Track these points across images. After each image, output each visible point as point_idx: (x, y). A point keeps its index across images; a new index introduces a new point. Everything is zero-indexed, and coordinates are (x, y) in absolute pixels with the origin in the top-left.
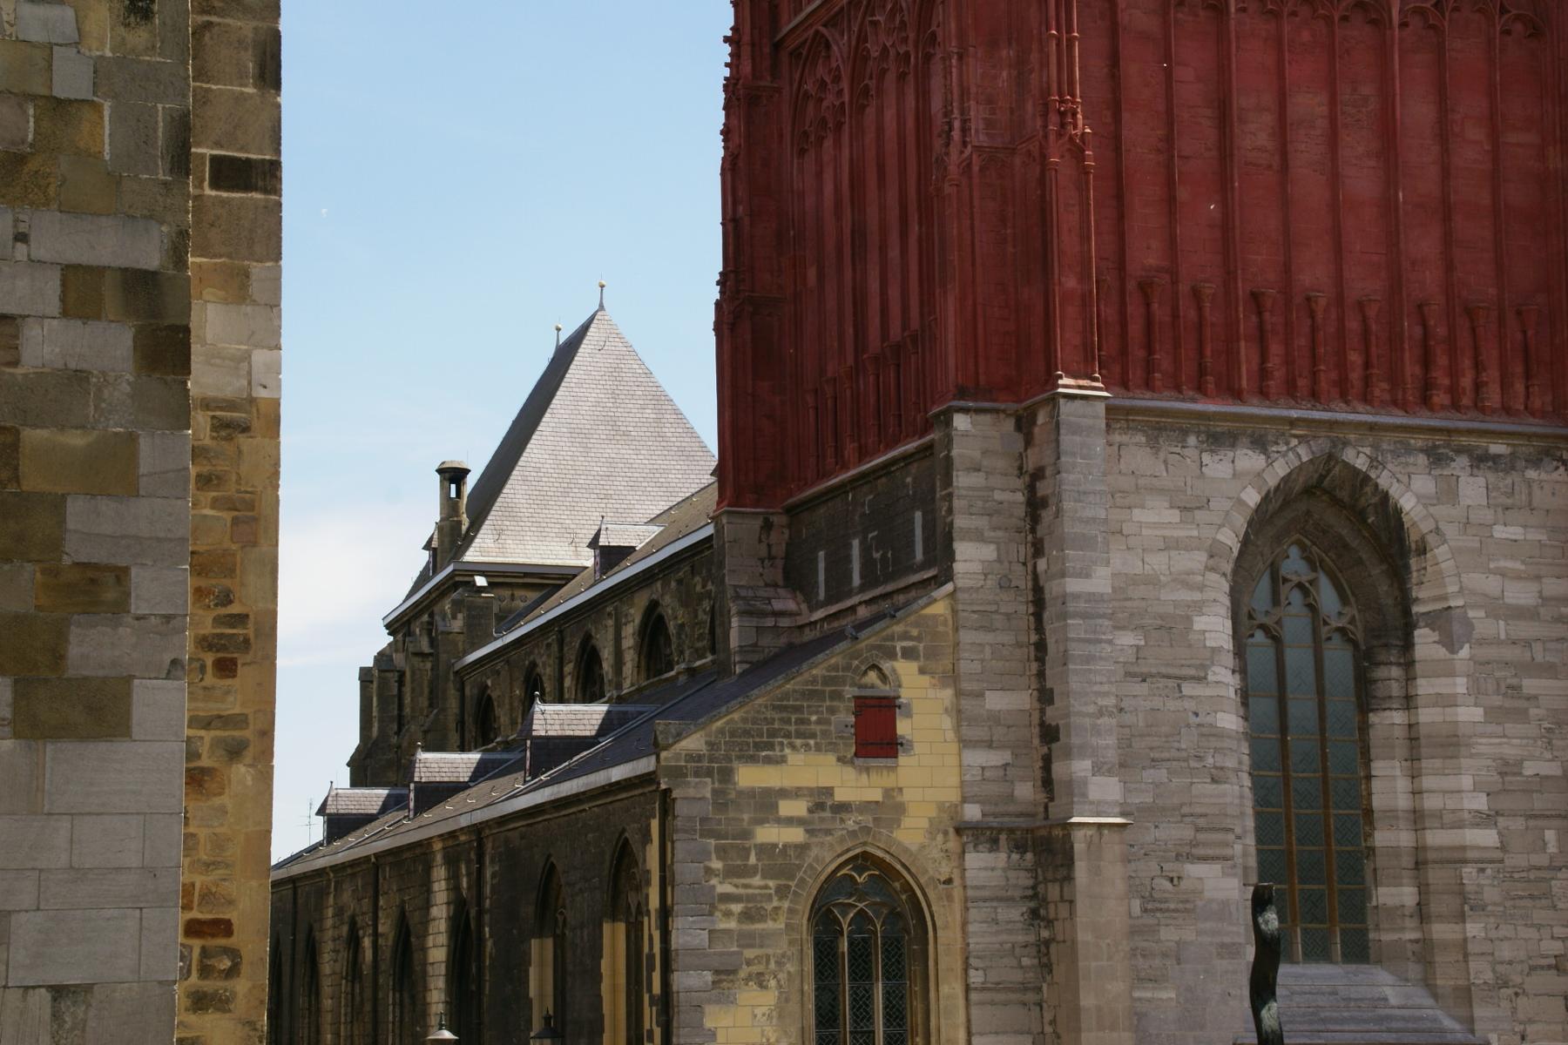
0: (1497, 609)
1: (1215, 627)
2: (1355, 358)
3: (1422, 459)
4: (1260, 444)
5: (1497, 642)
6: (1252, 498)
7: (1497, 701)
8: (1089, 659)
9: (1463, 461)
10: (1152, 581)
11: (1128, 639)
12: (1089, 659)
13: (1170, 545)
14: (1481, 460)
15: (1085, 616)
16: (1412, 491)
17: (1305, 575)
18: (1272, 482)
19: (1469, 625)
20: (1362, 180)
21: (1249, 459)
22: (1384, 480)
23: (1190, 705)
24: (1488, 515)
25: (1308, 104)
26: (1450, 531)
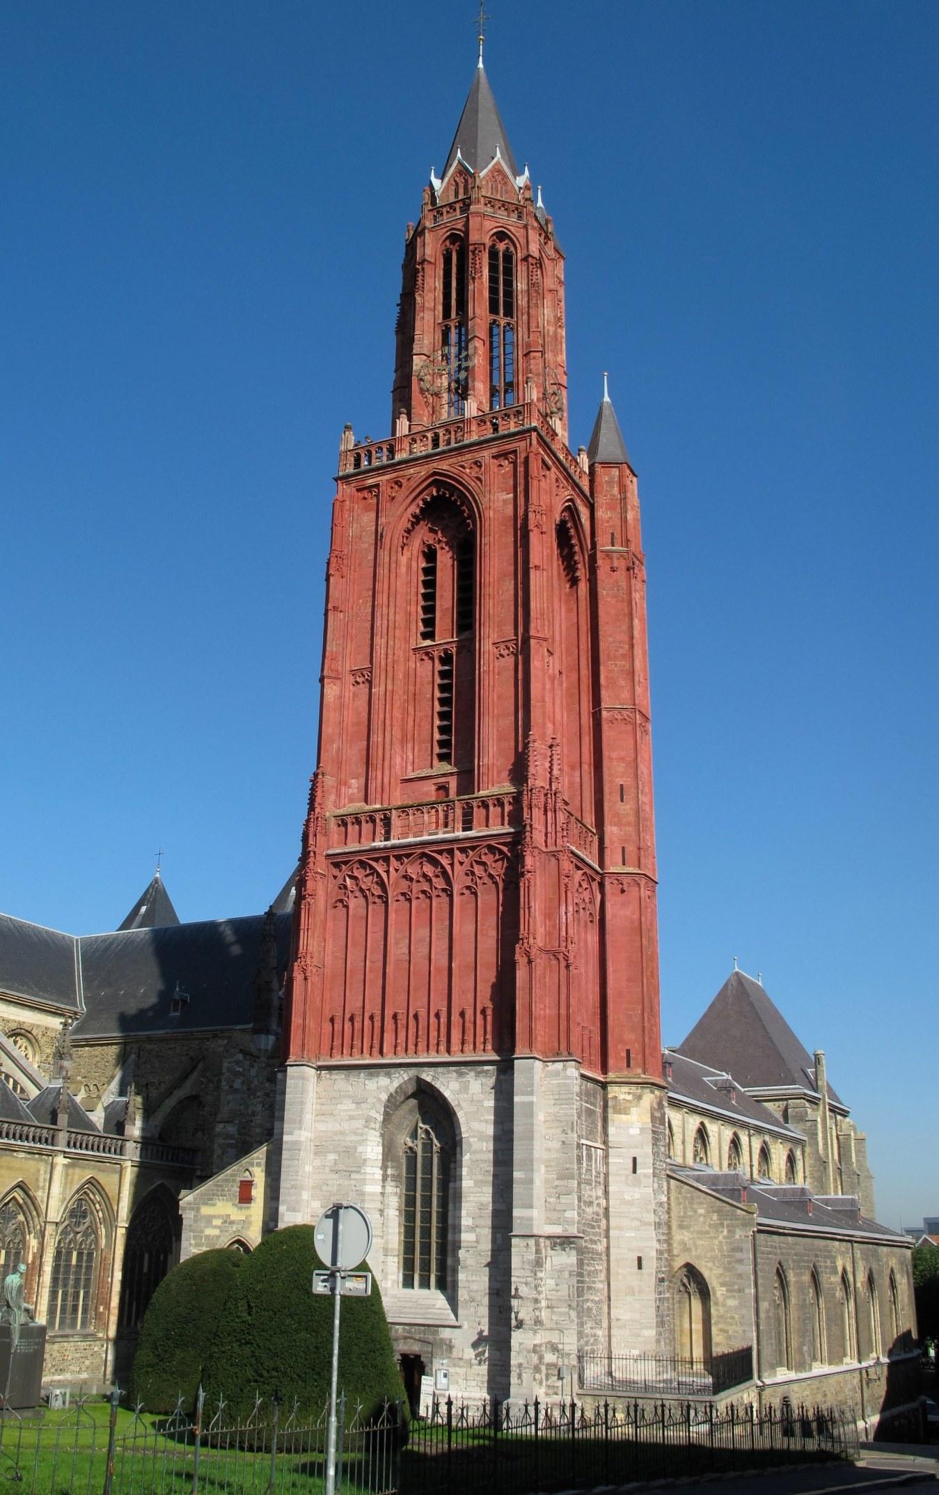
0: (481, 1137)
1: (373, 1150)
2: (433, 1034)
3: (455, 1075)
4: (388, 1075)
5: (482, 1151)
6: (384, 1097)
7: (480, 1177)
8: (289, 1166)
9: (472, 1074)
10: (342, 1133)
11: (332, 1157)
12: (289, 1166)
13: (351, 1118)
14: (478, 1074)
15: (289, 1150)
16: (449, 1086)
17: (427, 1127)
18: (392, 1090)
19: (470, 1145)
20: (440, 960)
21: (383, 1081)
22: (438, 1085)
23: (353, 1182)
24: (482, 1097)
25: (421, 933)
26: (464, 1104)
